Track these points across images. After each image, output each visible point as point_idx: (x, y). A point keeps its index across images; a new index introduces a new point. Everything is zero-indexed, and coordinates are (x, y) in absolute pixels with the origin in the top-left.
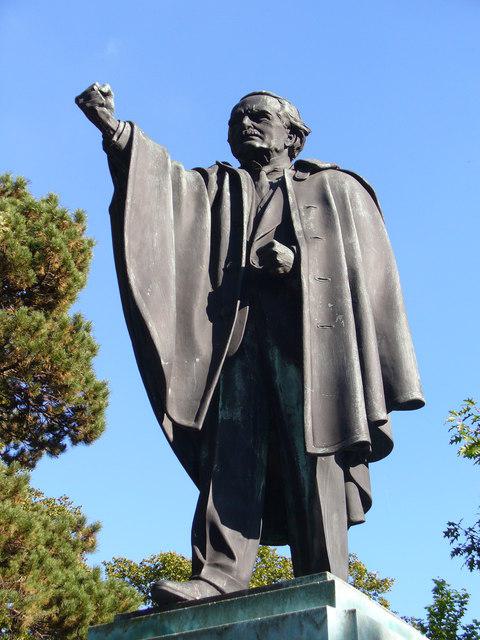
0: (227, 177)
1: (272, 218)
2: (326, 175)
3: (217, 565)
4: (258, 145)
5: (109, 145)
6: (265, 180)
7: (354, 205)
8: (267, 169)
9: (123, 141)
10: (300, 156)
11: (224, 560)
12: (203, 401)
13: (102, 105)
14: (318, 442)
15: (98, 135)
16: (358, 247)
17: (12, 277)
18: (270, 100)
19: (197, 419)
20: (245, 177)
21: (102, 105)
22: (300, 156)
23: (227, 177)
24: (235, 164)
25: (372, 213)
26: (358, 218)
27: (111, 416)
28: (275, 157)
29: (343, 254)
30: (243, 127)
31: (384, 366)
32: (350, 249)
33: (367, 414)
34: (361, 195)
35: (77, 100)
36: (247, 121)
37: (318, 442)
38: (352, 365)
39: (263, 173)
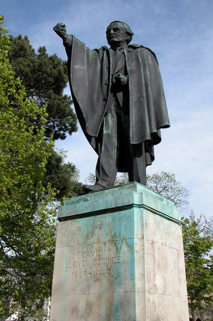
0: (105, 52)
1: (120, 65)
2: (138, 50)
3: (103, 180)
4: (115, 40)
5: (65, 44)
6: (118, 52)
7: (148, 59)
8: (119, 48)
9: (69, 42)
10: (131, 43)
11: (105, 178)
12: (99, 125)
13: (62, 30)
14: (134, 140)
15: (61, 40)
16: (148, 74)
17: (62, 84)
18: (119, 24)
19: (96, 134)
20: (111, 51)
21: (62, 30)
22: (131, 43)
23: (105, 52)
24: (109, 47)
25: (153, 62)
26: (148, 64)
27: (79, 129)
28: (122, 44)
29: (143, 76)
30: (111, 34)
31: (156, 118)
32: (145, 75)
33: (144, 262)
34: (150, 57)
35: (54, 29)
36: (112, 31)
37: (134, 140)
38: (145, 115)
39: (117, 50)
